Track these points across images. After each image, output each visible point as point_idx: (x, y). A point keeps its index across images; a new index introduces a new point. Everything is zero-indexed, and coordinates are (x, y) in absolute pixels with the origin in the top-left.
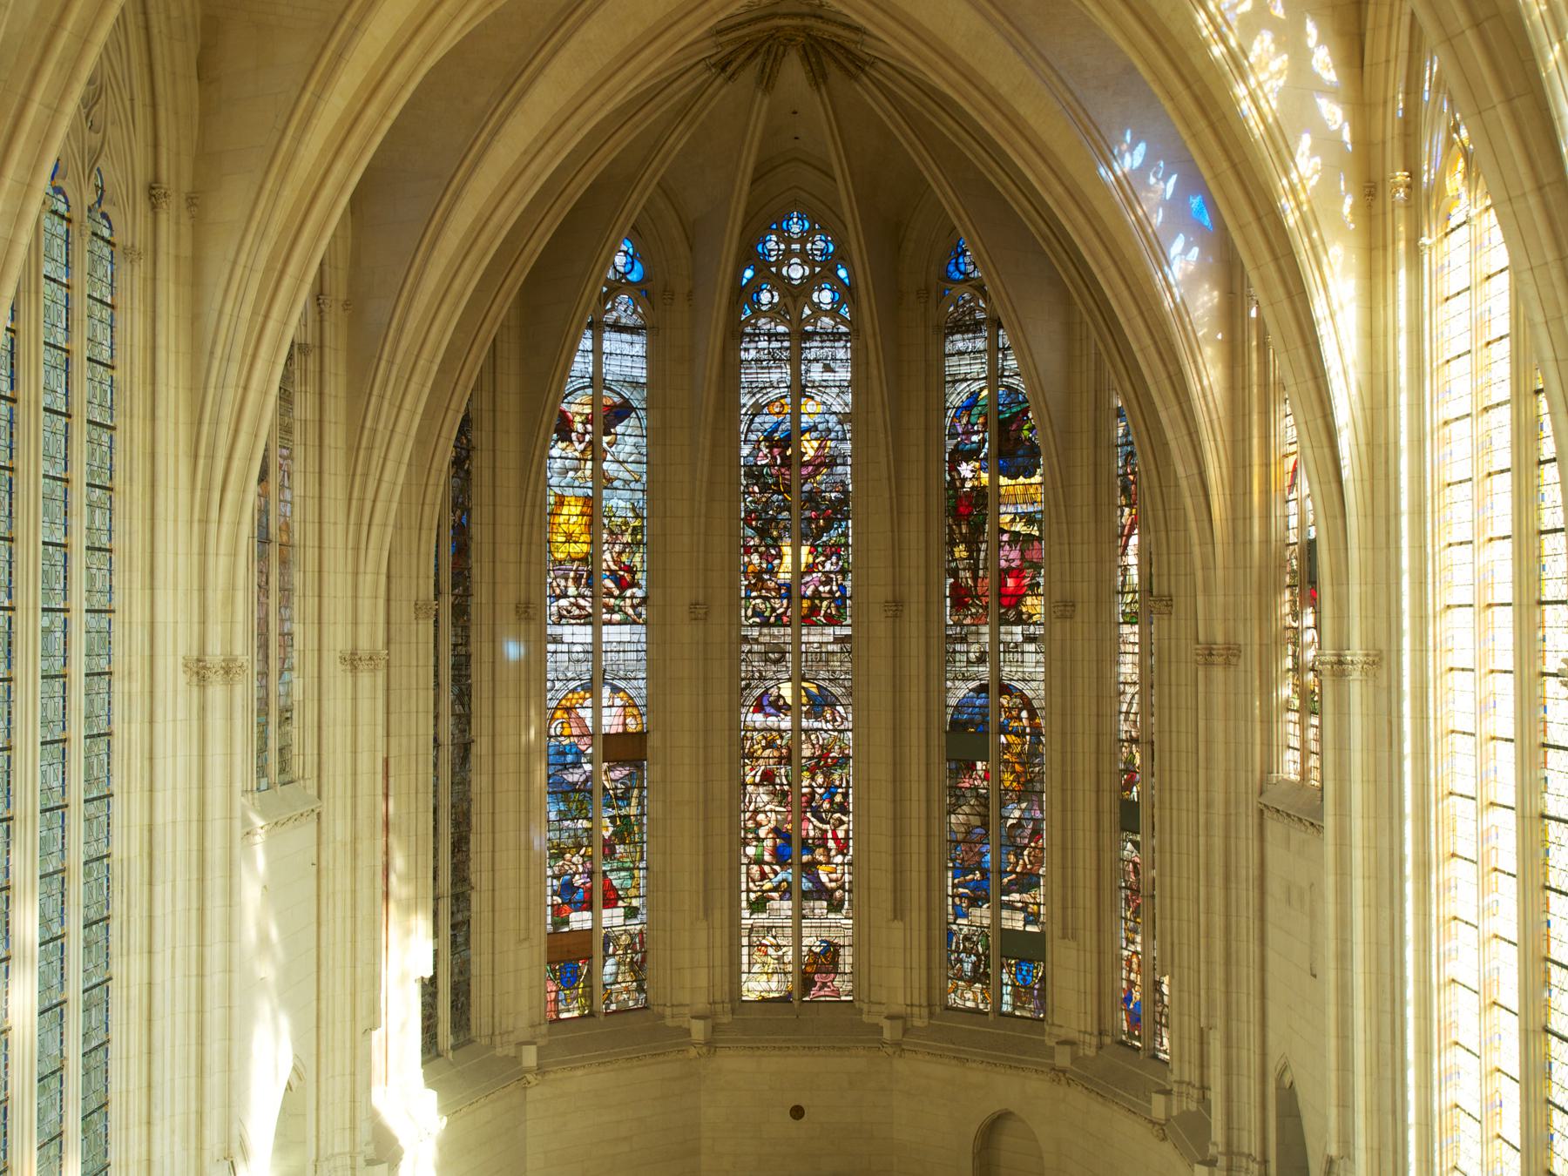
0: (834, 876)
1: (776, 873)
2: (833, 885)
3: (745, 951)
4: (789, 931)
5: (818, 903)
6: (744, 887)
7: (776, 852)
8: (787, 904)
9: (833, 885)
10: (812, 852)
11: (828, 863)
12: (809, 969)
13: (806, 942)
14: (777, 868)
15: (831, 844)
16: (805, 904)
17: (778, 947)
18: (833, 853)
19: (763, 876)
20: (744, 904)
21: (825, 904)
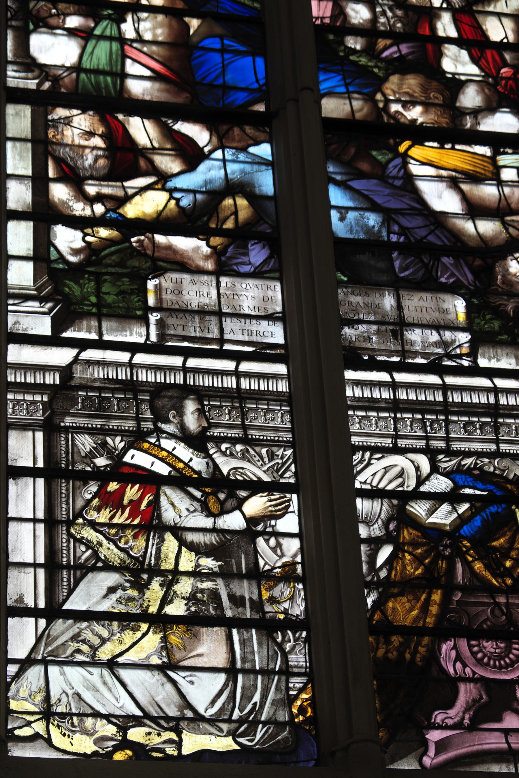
0: (489, 191)
1: (191, 156)
2: (487, 227)
3: (26, 498)
4: (276, 421)
5: (417, 304)
6: (19, 195)
7: (179, 62)
8: (255, 295)
9: (487, 227)
10: (365, 81)
11: (453, 131)
12: (403, 610)
13: (372, 473)
14: (199, 134)
15: (456, 62)
16: (352, 299)
17: (219, 491)
18: (470, 98)
19: (125, 160)
20: (21, 274)
21: (458, 307)
